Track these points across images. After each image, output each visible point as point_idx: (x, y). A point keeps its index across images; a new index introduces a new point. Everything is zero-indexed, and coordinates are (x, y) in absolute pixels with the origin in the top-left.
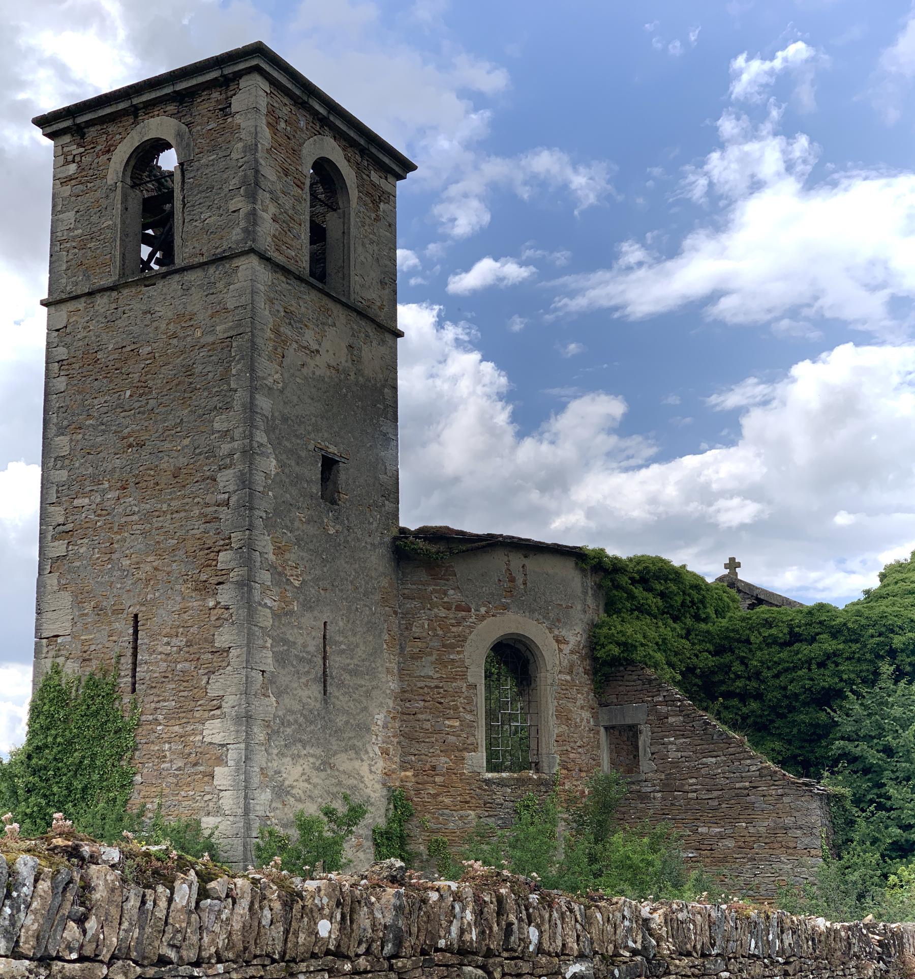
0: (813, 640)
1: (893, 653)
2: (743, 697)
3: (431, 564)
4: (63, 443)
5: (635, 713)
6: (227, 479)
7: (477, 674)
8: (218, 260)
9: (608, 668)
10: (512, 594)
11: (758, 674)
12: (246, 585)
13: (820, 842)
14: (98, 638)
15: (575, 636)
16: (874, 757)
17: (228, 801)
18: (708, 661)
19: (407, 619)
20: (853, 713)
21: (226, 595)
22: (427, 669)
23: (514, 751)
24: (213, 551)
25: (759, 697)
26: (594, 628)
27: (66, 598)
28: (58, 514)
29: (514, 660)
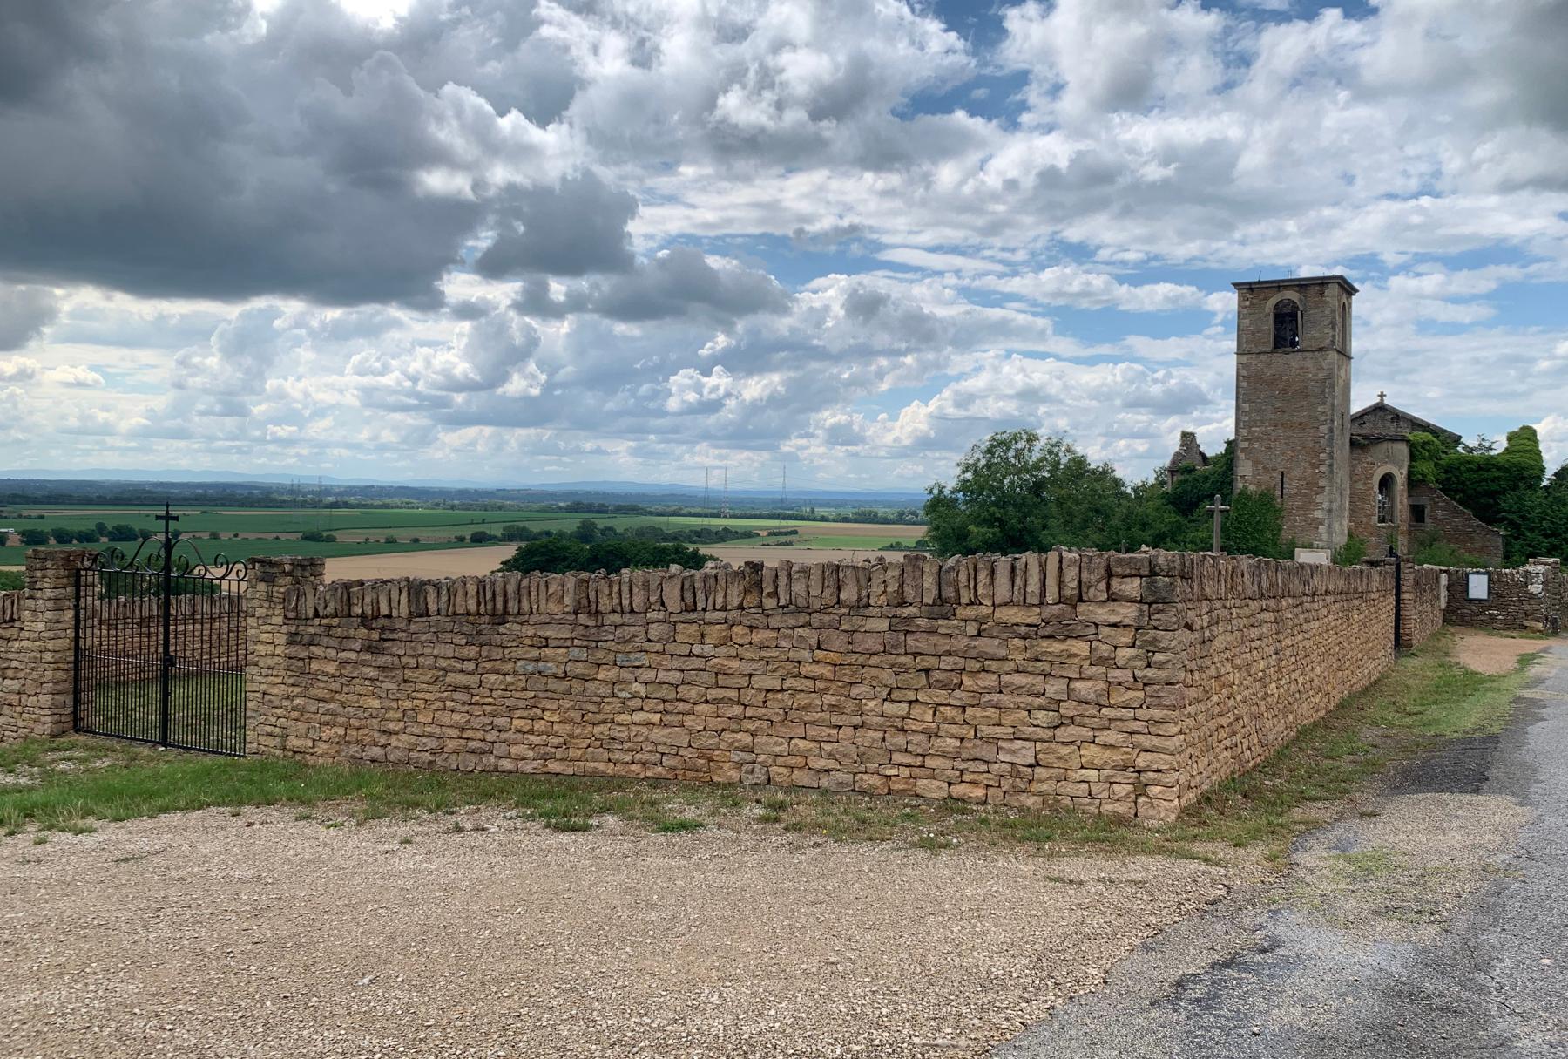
0: (1488, 470)
1: (1523, 478)
2: (1456, 491)
3: (1363, 448)
4: (1246, 407)
5: (1424, 500)
6: (1324, 429)
7: (1376, 488)
8: (1321, 350)
9: (1413, 483)
10: (1389, 458)
11: (1463, 483)
12: (1331, 466)
13: (1501, 552)
14: (1266, 478)
15: (1405, 471)
16: (1519, 521)
17: (1325, 537)
18: (1443, 476)
19: (1353, 467)
20: (1508, 501)
21: (1323, 468)
22: (1360, 486)
23: (1386, 515)
24: (1316, 454)
25: (1462, 491)
26: (1410, 467)
27: (1250, 463)
28: (1244, 432)
29: (1386, 482)
